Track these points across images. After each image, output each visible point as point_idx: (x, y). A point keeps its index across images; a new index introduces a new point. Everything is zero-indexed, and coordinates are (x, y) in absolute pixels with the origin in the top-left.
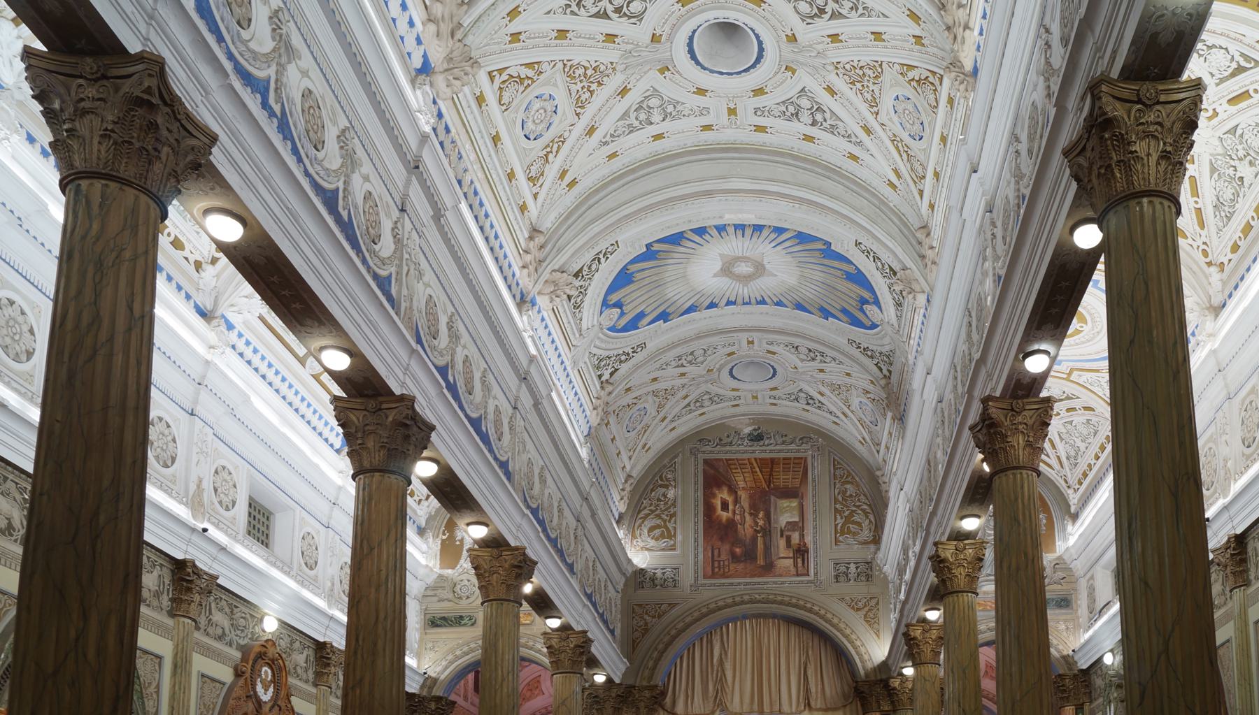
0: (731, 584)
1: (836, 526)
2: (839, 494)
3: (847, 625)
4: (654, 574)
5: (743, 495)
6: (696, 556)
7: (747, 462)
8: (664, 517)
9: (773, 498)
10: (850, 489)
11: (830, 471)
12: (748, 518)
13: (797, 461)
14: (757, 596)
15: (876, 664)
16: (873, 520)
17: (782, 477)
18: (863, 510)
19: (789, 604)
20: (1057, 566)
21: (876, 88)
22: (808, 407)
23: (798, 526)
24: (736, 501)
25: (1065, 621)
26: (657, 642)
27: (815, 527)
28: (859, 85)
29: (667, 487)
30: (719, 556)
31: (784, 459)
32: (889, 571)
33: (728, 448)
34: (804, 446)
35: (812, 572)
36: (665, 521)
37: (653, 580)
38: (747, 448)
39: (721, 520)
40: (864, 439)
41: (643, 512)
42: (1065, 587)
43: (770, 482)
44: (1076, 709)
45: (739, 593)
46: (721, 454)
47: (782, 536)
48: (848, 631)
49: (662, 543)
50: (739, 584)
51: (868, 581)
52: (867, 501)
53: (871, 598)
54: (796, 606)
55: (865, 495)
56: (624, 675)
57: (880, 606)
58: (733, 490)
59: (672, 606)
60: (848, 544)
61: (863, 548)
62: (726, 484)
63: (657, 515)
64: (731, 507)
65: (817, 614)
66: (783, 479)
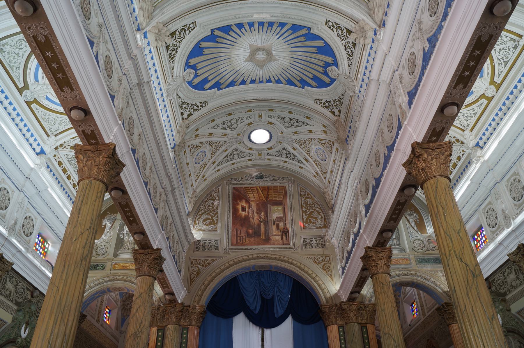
0: (247, 249)
1: (303, 219)
2: (304, 203)
3: (313, 272)
4: (205, 243)
5: (254, 205)
6: (228, 234)
7: (255, 188)
8: (212, 214)
9: (269, 205)
10: (310, 201)
11: (298, 193)
12: (256, 215)
13: (280, 188)
14: (261, 255)
15: (332, 295)
16: (323, 216)
17: (273, 195)
18: (317, 211)
19: (279, 260)
20: (429, 241)
21: (309, 146)
22: (287, 160)
23: (283, 219)
24: (250, 207)
26: (204, 280)
27: (292, 219)
28: (303, 146)
29: (214, 200)
30: (240, 234)
31: (274, 187)
32: (335, 241)
33: (246, 182)
34: (284, 181)
35: (291, 242)
36: (212, 216)
37: (204, 247)
38: (255, 182)
39: (241, 216)
40: (317, 173)
41: (201, 212)
43: (267, 198)
45: (251, 253)
46: (241, 184)
47: (274, 224)
48: (314, 275)
49: (210, 227)
50: (251, 249)
51: (323, 247)
52: (319, 207)
53: (326, 257)
54: (283, 261)
55: (317, 204)
56: (184, 299)
57: (331, 261)
58: (248, 202)
59: (213, 260)
60: (311, 228)
61: (318, 231)
62: (244, 199)
63: (208, 214)
64: (247, 210)
65: (295, 265)
66: (274, 196)
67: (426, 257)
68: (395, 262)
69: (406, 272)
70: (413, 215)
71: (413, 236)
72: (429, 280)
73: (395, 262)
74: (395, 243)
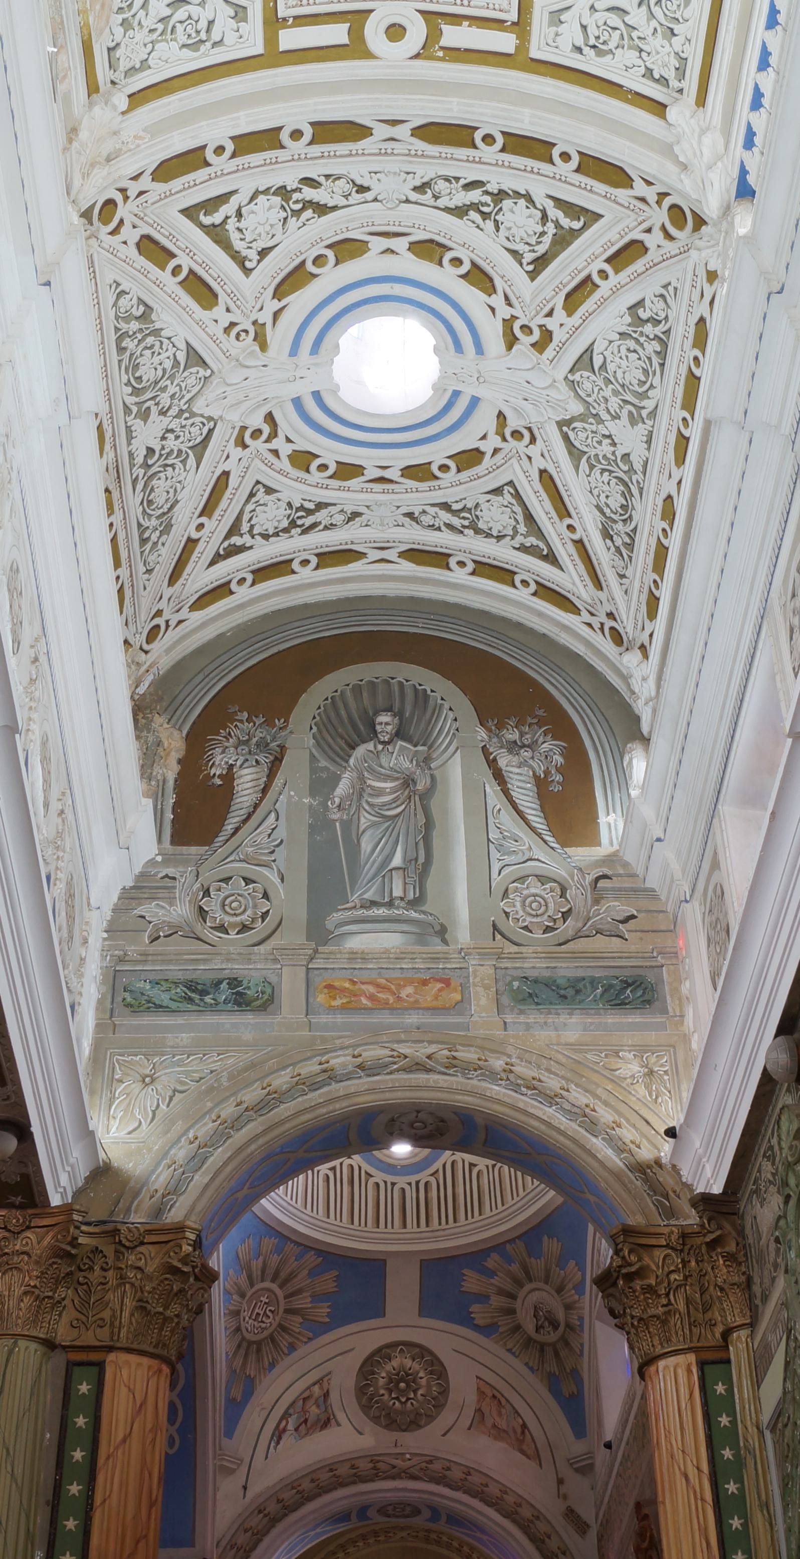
20: (602, 884)
25: (641, 1051)
42: (634, 944)
44: (702, 1365)
67: (566, 970)
68: (371, 998)
69: (420, 1052)
70: (531, 746)
71: (512, 859)
72: (552, 1099)
73: (371, 998)
74: (398, 892)
